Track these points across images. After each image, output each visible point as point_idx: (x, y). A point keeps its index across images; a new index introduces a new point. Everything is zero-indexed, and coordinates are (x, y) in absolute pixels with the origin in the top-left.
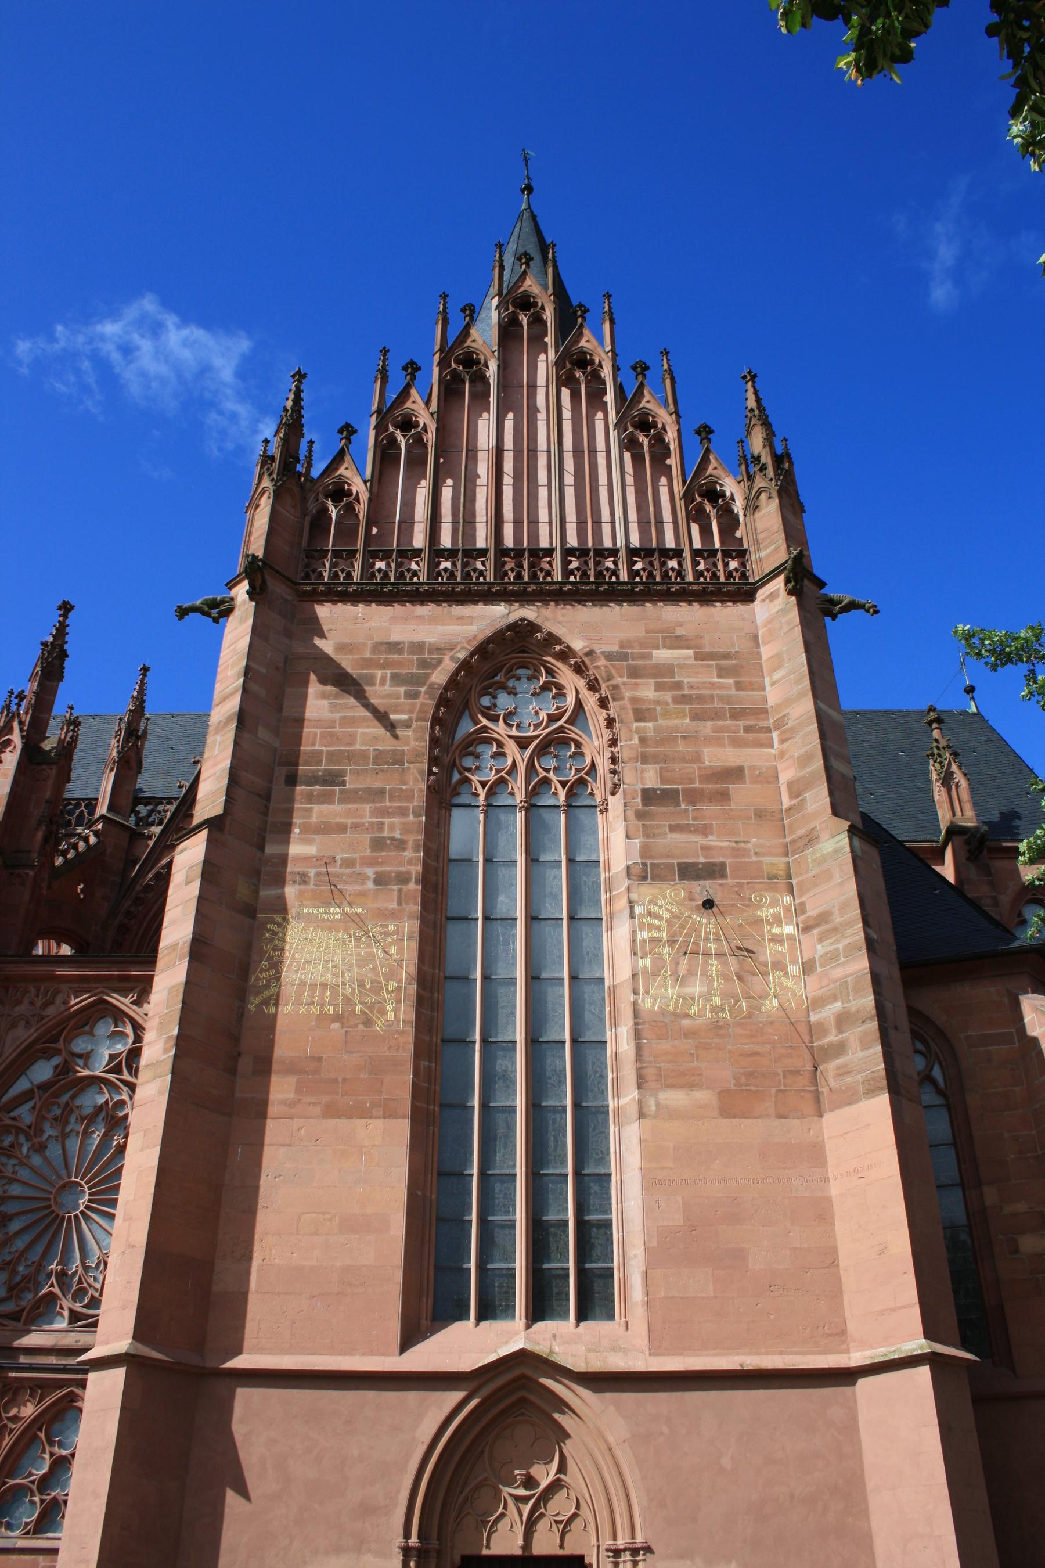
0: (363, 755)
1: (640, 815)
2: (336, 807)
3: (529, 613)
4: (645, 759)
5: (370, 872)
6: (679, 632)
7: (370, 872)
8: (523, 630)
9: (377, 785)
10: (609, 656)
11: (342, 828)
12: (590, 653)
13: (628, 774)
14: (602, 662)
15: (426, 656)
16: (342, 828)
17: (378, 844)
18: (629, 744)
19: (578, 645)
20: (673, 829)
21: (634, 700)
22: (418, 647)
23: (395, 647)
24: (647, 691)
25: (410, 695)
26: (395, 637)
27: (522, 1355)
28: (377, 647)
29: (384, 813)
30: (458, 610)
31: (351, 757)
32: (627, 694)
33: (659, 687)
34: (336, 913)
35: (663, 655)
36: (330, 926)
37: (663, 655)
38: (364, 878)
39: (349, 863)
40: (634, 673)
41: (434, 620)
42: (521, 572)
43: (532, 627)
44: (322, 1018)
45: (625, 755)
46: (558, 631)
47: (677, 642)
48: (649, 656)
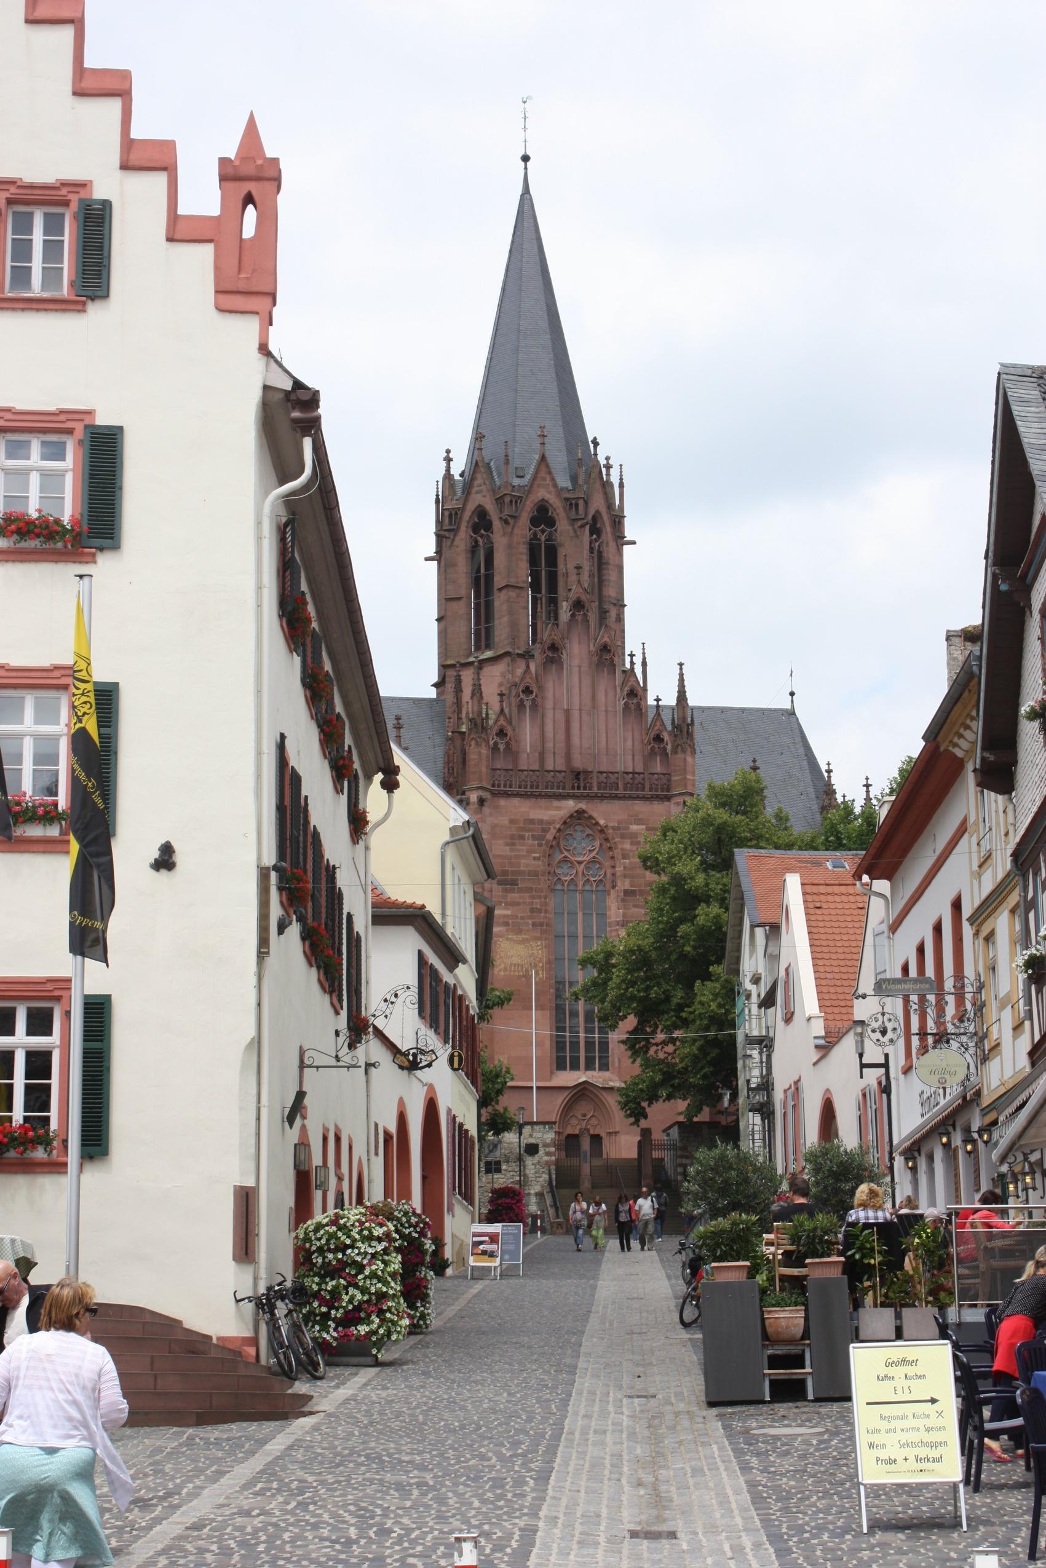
0: (524, 872)
1: (623, 900)
2: (516, 895)
3: (582, 805)
4: (625, 876)
5: (530, 922)
6: (640, 816)
7: (530, 922)
8: (580, 813)
9: (529, 885)
10: (613, 828)
11: (518, 904)
12: (606, 826)
13: (619, 883)
14: (611, 831)
15: (544, 826)
16: (518, 904)
17: (532, 910)
18: (619, 869)
19: (602, 822)
20: (635, 906)
21: (622, 849)
22: (541, 822)
23: (532, 821)
24: (627, 846)
25: (540, 845)
26: (532, 817)
27: (585, 1082)
28: (525, 820)
29: (533, 897)
30: (556, 803)
31: (519, 873)
32: (620, 846)
33: (632, 844)
34: (520, 937)
35: (634, 828)
36: (519, 942)
37: (634, 828)
38: (528, 924)
39: (522, 918)
40: (623, 837)
41: (547, 808)
42: (578, 781)
43: (584, 812)
44: (519, 977)
45: (618, 874)
46: (595, 815)
47: (639, 822)
48: (628, 828)
